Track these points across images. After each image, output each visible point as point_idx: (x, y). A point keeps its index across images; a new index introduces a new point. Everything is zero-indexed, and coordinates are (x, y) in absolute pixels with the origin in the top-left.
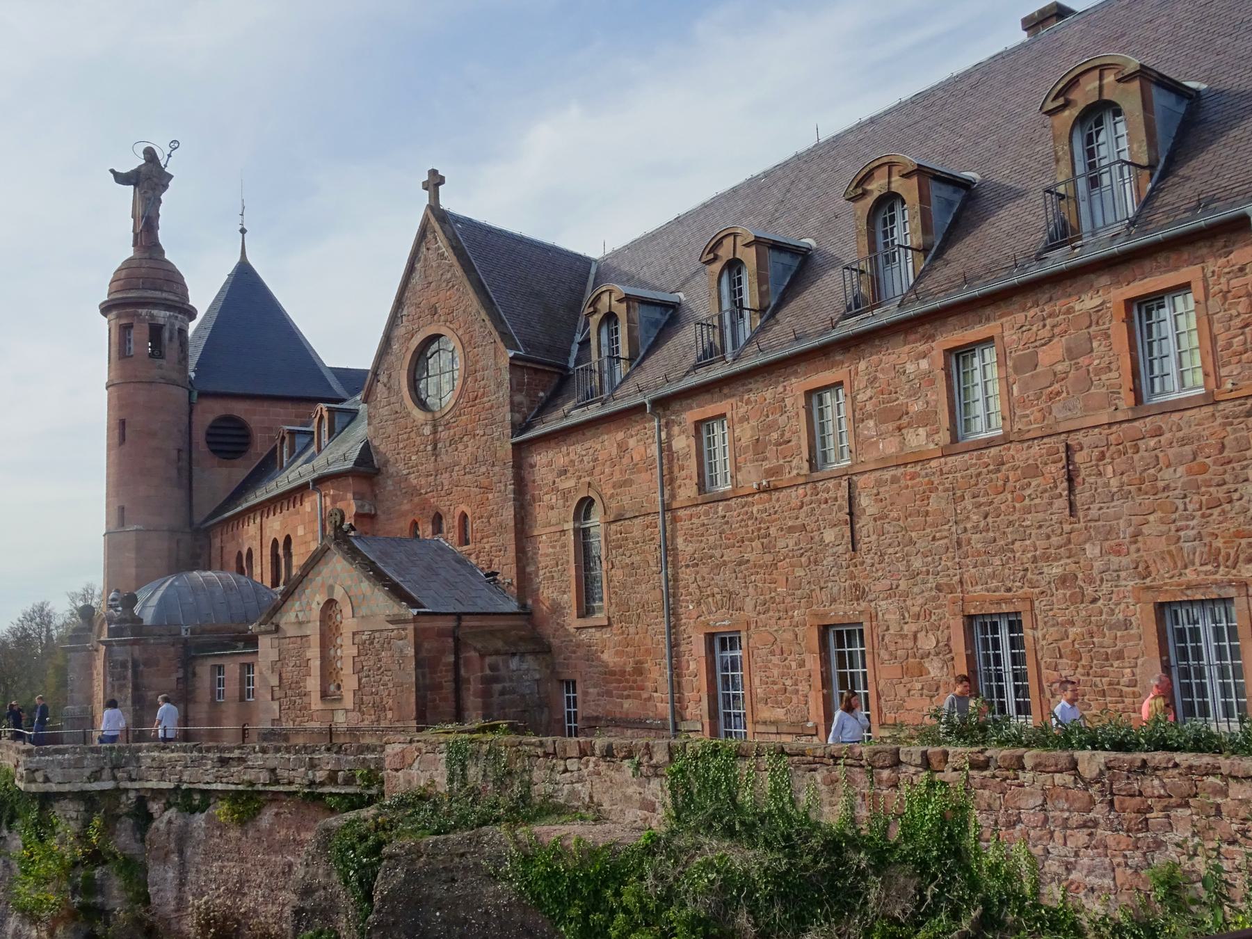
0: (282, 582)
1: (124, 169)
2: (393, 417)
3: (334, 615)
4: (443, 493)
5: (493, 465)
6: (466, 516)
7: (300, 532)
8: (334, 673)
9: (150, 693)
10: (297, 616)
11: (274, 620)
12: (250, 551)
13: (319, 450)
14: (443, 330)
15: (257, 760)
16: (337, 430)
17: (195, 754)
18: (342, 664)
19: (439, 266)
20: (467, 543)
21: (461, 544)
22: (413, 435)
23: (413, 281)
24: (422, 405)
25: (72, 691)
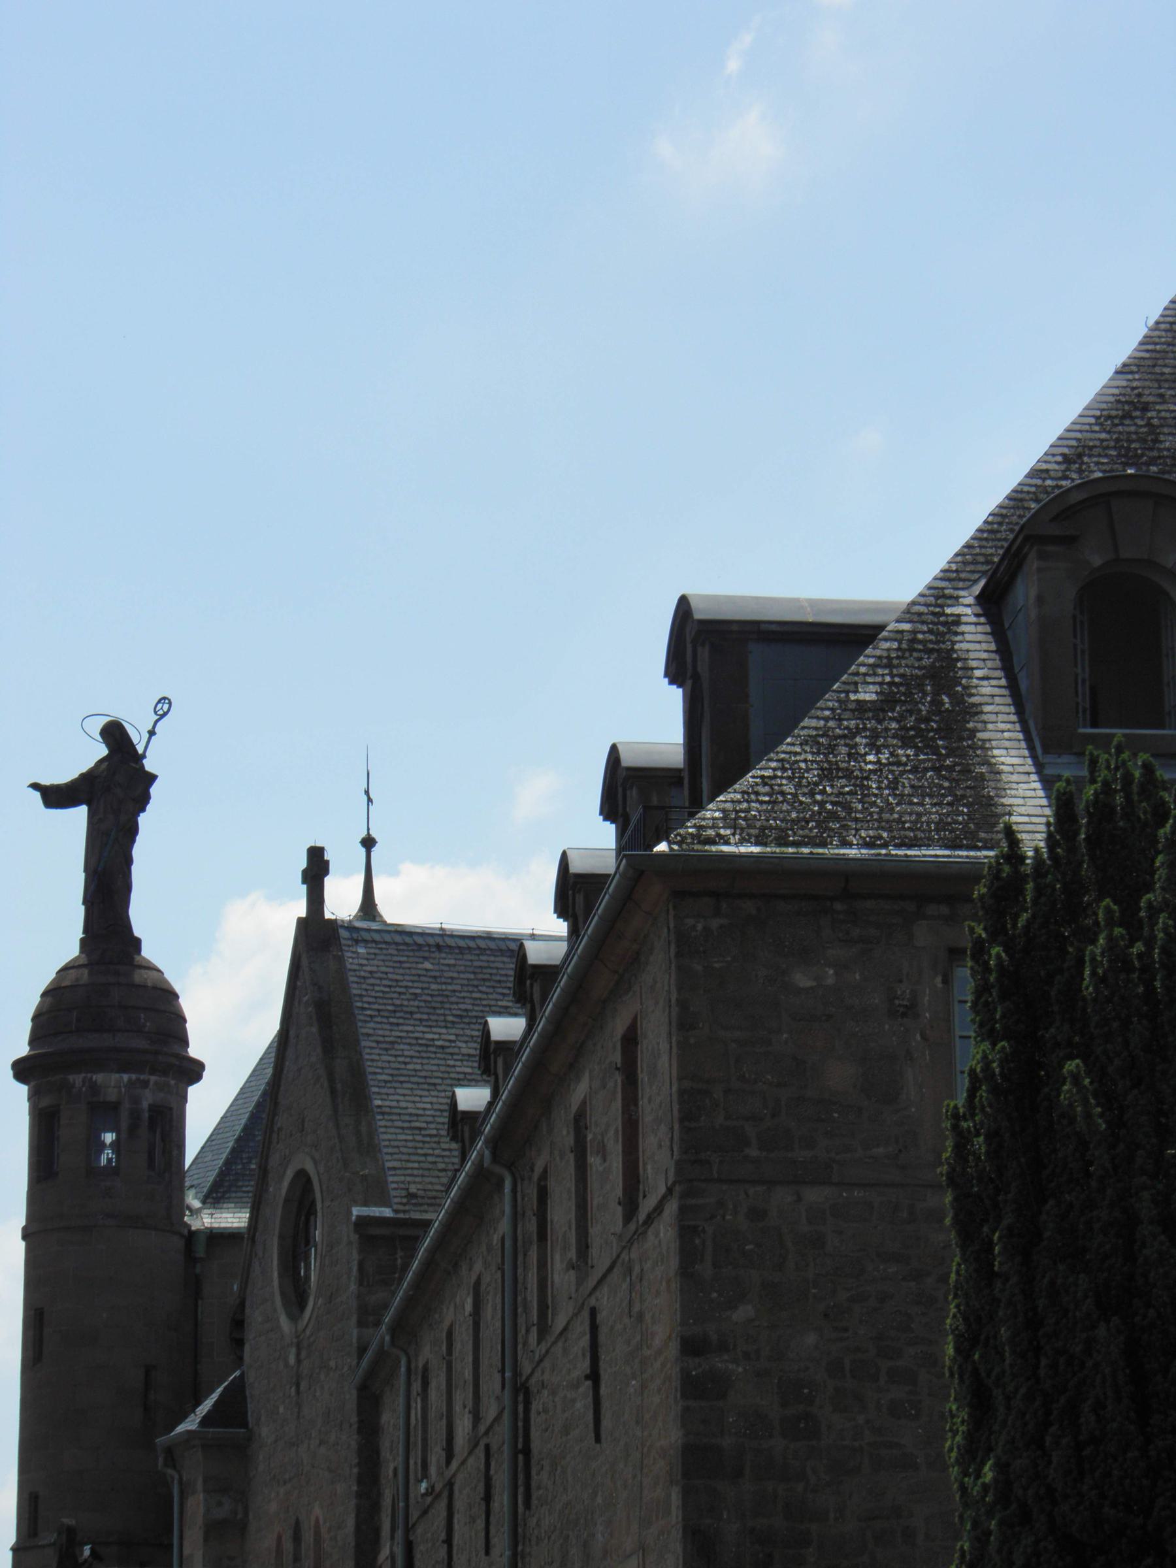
1: (64, 774)
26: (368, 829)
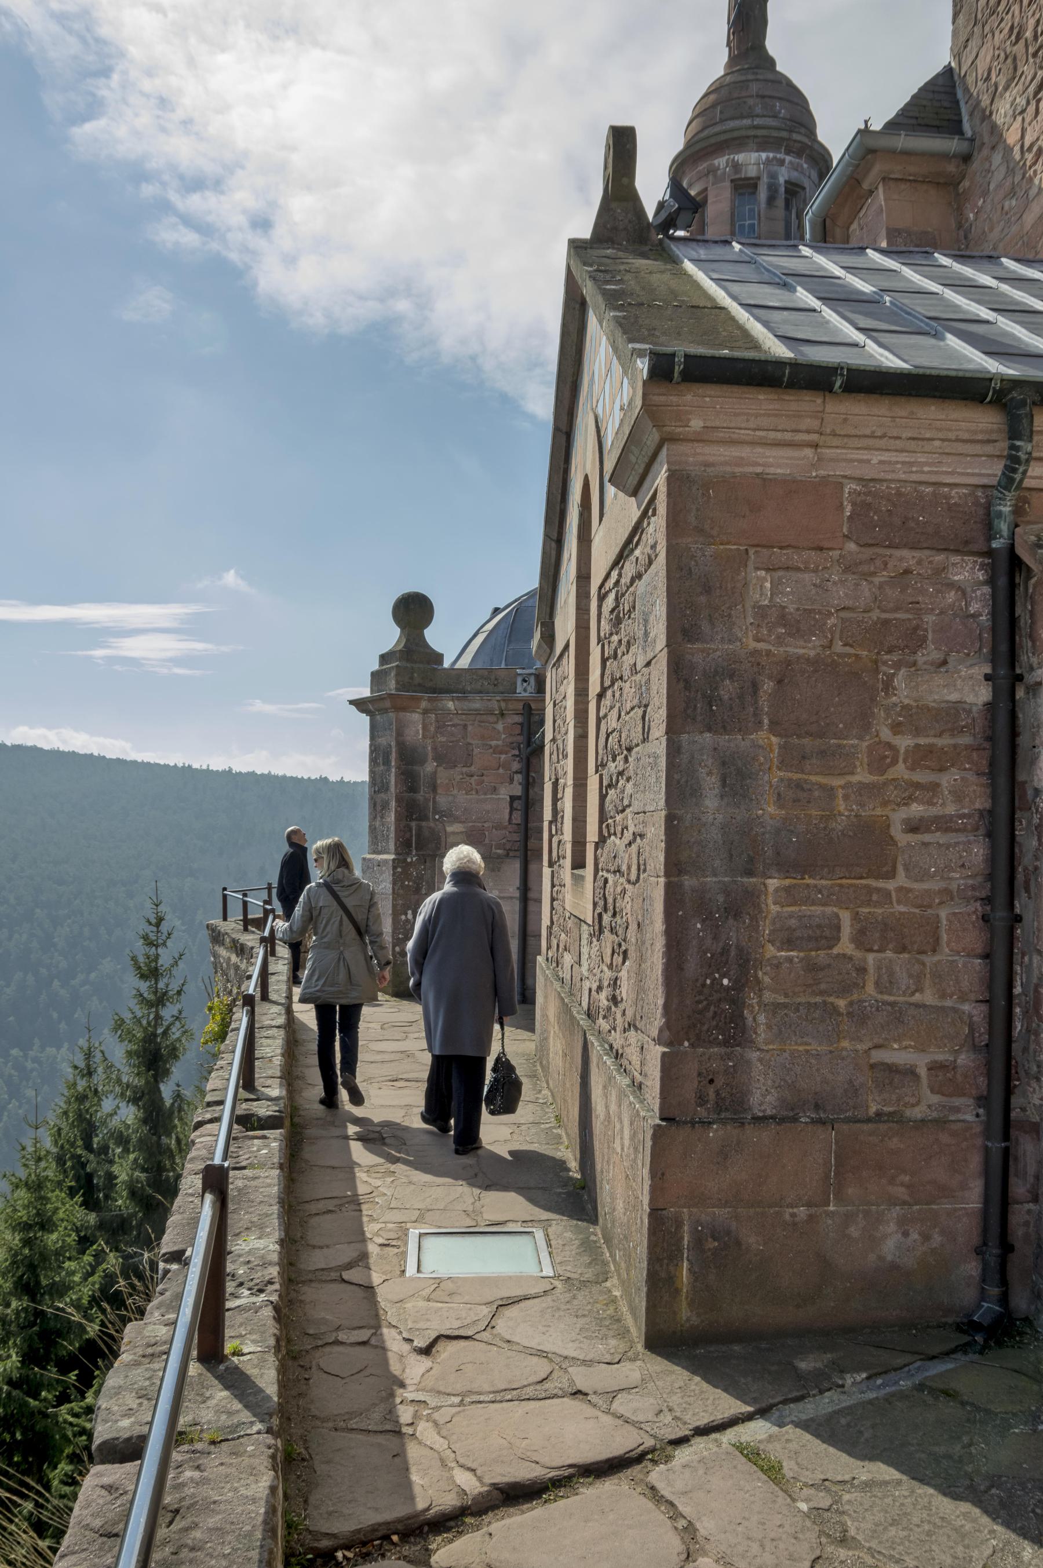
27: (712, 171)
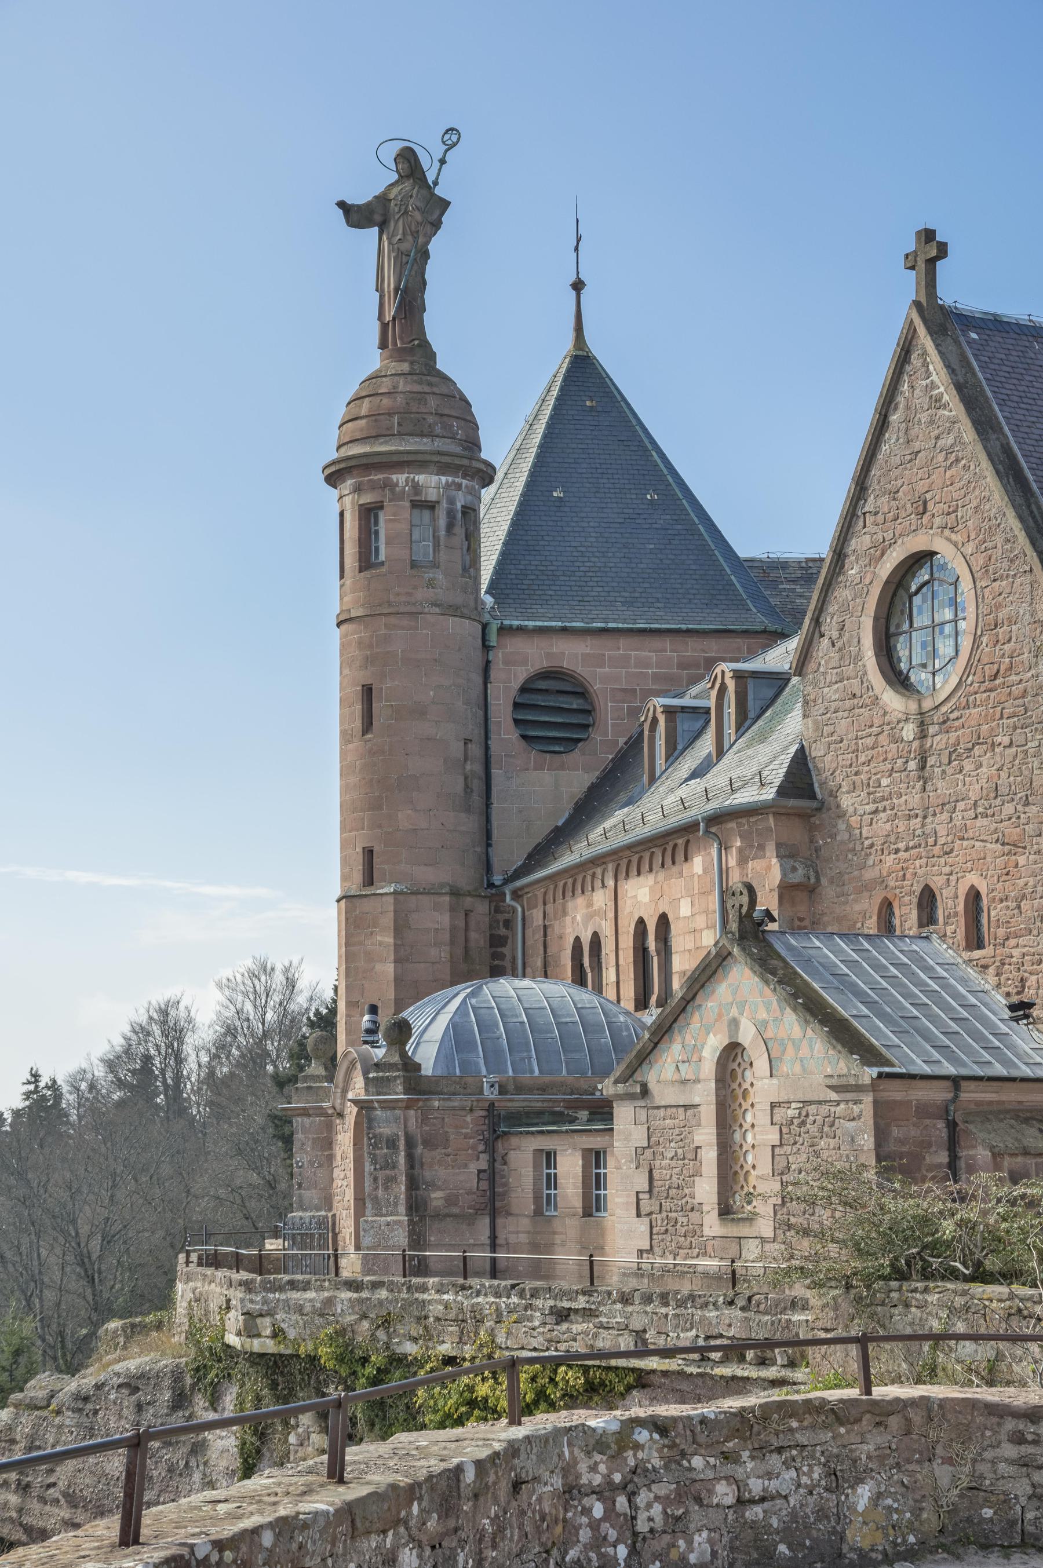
0: (654, 999)
1: (360, 197)
2: (848, 704)
3: (739, 1071)
4: (937, 850)
5: (1027, 804)
6: (974, 897)
7: (685, 909)
8: (742, 1174)
9: (433, 1195)
10: (677, 1066)
11: (638, 1076)
12: (596, 936)
13: (720, 753)
14: (939, 545)
15: (614, 1313)
16: (751, 715)
17: (515, 1299)
18: (755, 1157)
19: (932, 422)
20: (980, 946)
21: (969, 947)
22: (883, 739)
23: (885, 448)
24: (899, 680)
25: (300, 1185)
26: (578, 273)
27: (388, 485)
